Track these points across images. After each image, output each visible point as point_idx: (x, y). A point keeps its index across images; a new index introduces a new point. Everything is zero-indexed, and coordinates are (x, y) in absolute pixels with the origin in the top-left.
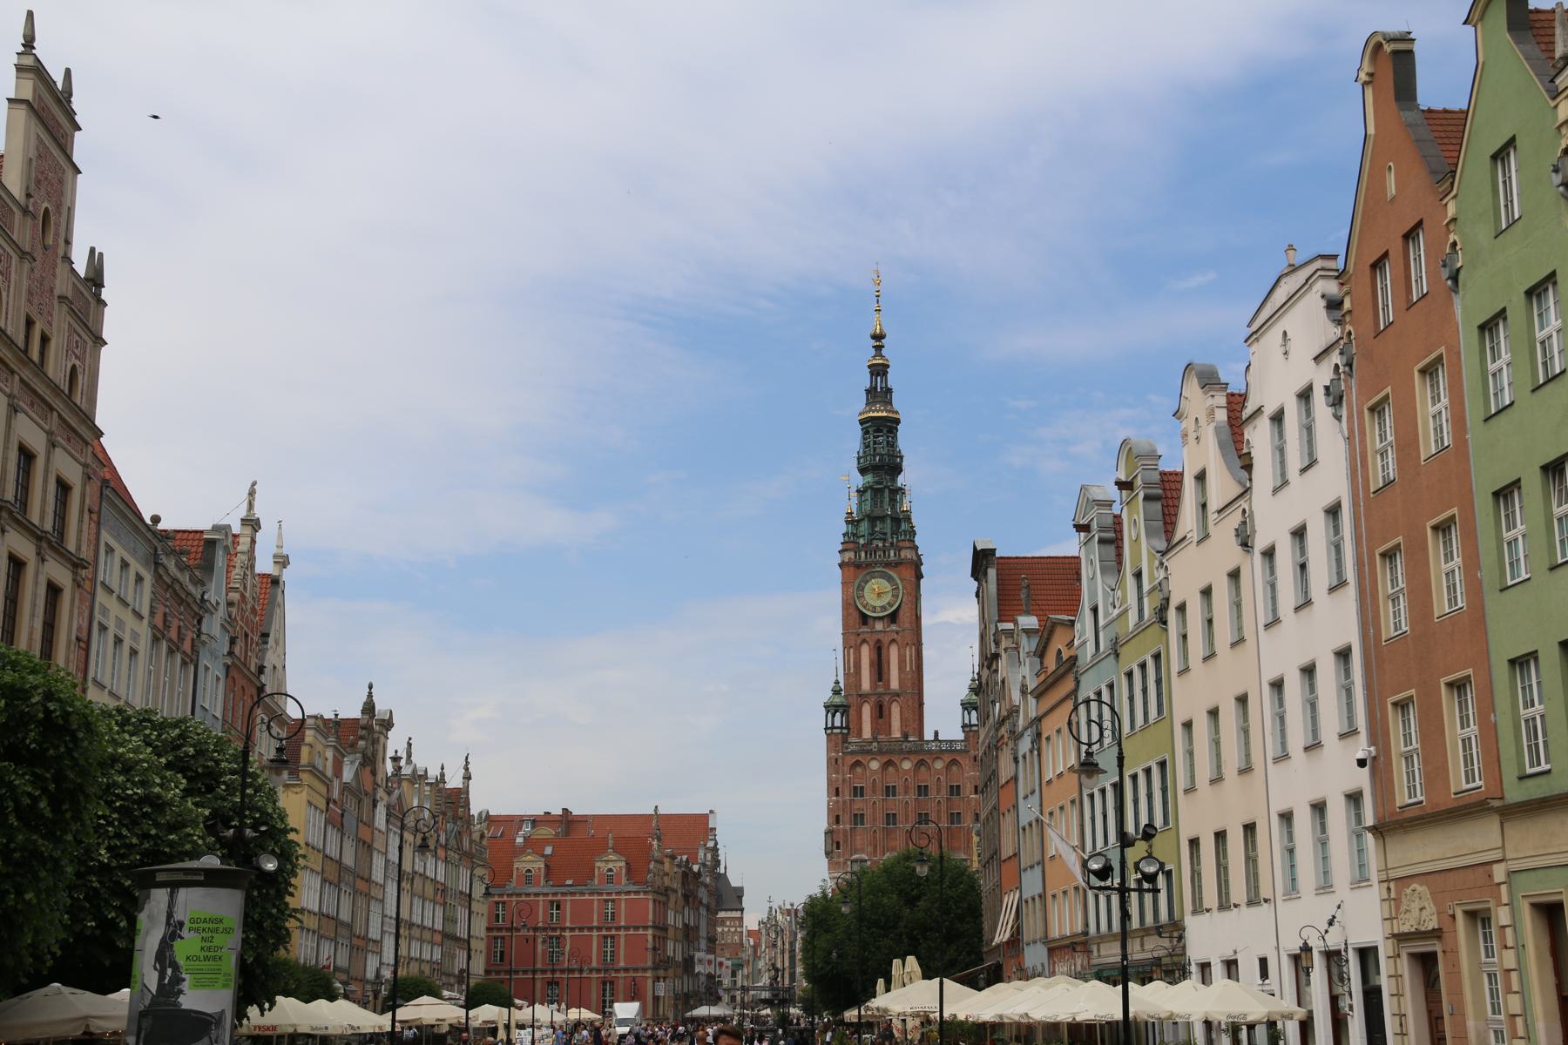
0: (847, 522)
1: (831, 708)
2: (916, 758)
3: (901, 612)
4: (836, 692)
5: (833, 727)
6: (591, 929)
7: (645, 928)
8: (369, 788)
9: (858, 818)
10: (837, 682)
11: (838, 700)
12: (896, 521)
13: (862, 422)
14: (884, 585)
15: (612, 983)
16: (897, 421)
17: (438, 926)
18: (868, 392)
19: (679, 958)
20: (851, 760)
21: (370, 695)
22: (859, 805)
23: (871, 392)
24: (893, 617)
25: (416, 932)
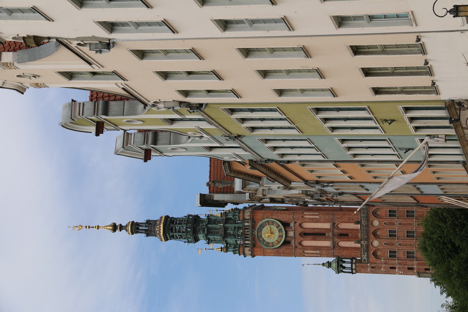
0: (227, 251)
1: (340, 269)
2: (372, 217)
3: (283, 220)
4: (329, 265)
5: (352, 269)
10: (323, 264)
11: (334, 265)
12: (227, 220)
14: (266, 229)
16: (167, 217)
18: (148, 235)
20: (372, 258)
22: (401, 254)
23: (149, 233)
24: (286, 225)
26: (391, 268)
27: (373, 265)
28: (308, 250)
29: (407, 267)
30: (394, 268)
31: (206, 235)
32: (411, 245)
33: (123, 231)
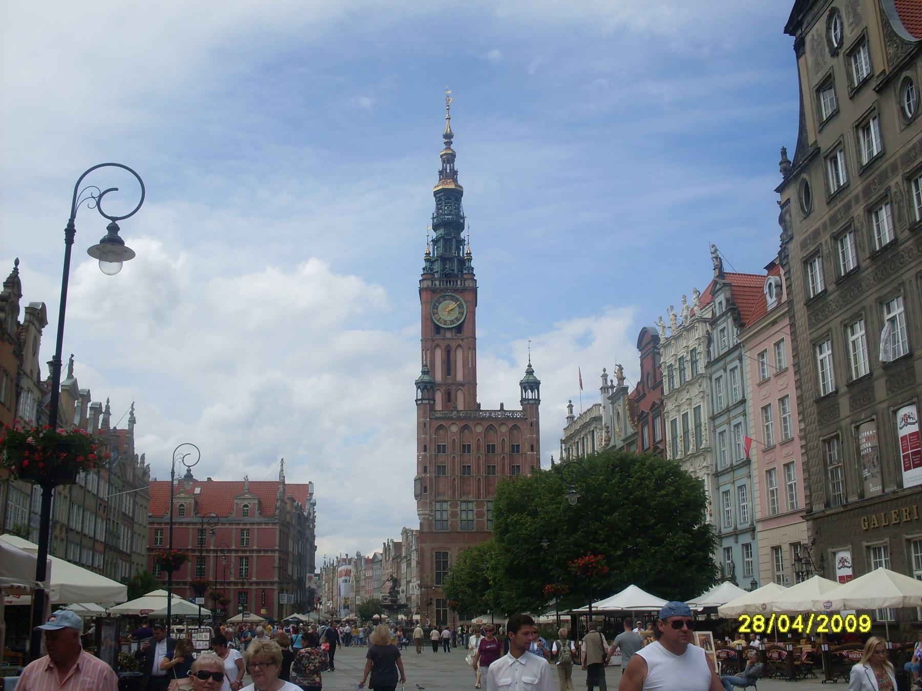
0: (426, 260)
3: (465, 325)
4: (423, 373)
6: (230, 551)
7: (273, 551)
8: (13, 372)
9: (441, 469)
11: (426, 378)
13: (436, 193)
14: (453, 305)
15: (246, 593)
17: (101, 537)
18: (441, 173)
19: (295, 577)
20: (436, 424)
21: (16, 271)
22: (442, 458)
24: (459, 329)
25: (72, 536)
26: (425, 446)
27: (428, 425)
28: (431, 354)
29: (428, 465)
30: (425, 450)
31: (443, 237)
32: (454, 470)
33: (445, 147)
